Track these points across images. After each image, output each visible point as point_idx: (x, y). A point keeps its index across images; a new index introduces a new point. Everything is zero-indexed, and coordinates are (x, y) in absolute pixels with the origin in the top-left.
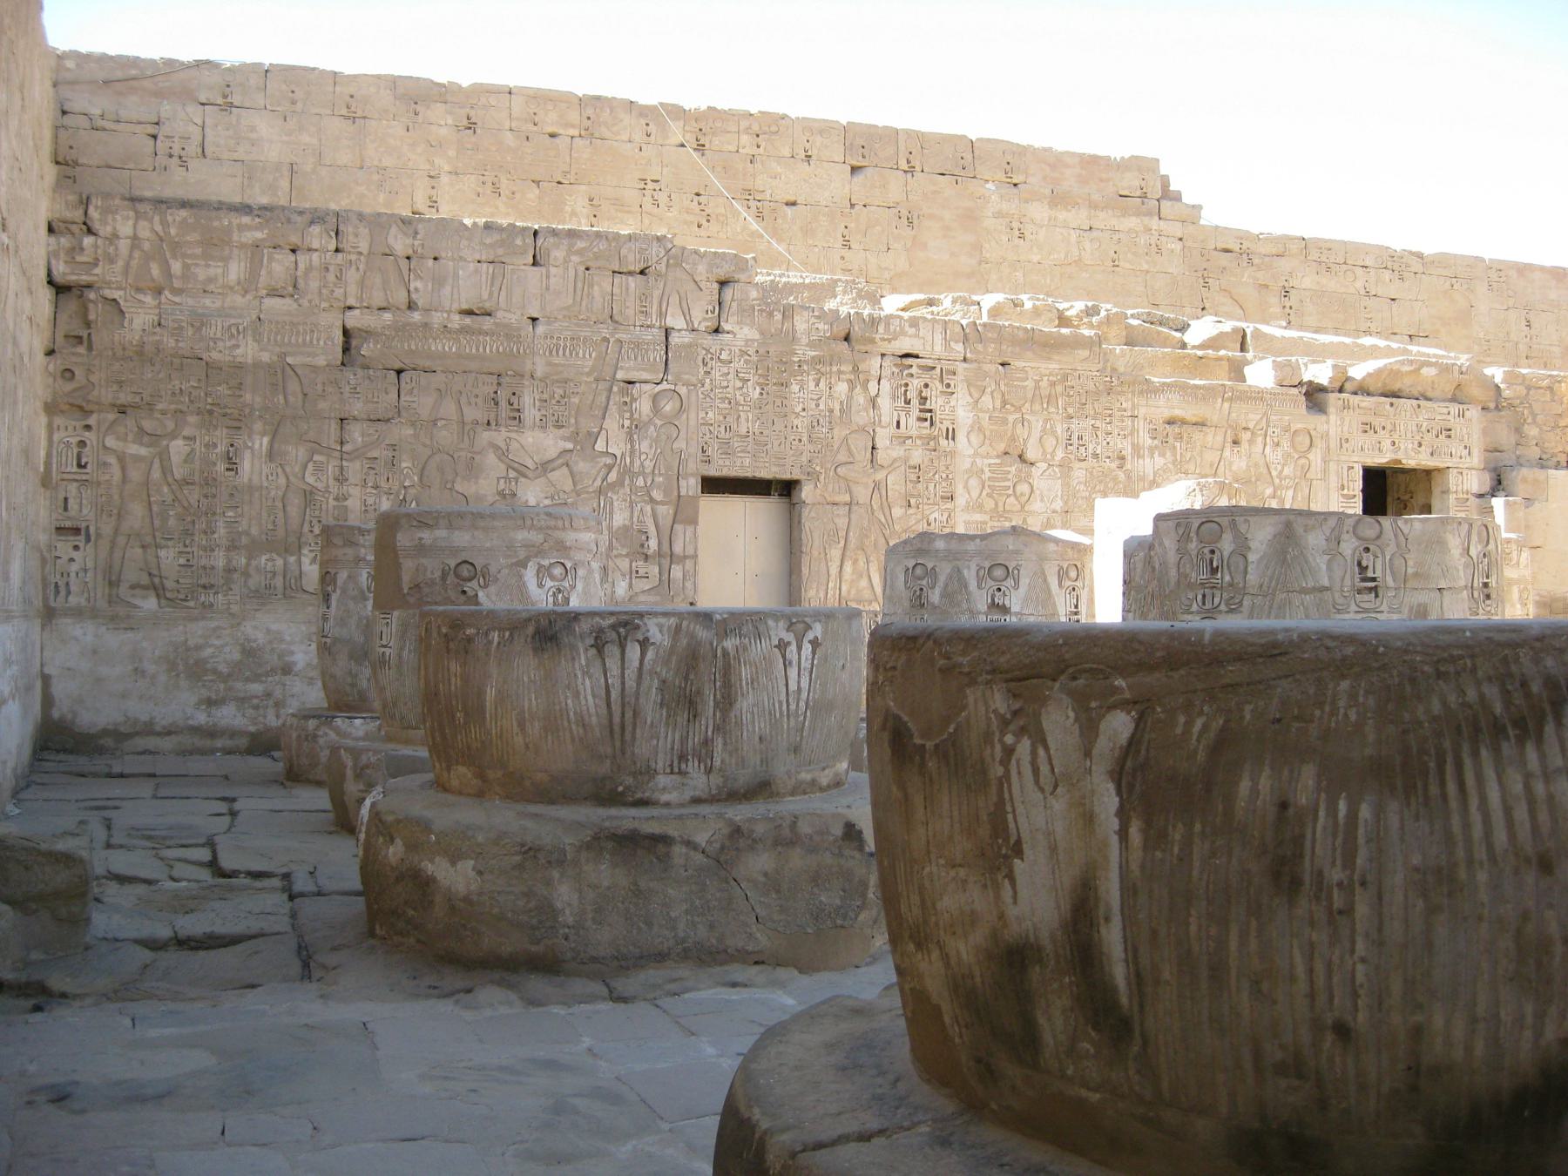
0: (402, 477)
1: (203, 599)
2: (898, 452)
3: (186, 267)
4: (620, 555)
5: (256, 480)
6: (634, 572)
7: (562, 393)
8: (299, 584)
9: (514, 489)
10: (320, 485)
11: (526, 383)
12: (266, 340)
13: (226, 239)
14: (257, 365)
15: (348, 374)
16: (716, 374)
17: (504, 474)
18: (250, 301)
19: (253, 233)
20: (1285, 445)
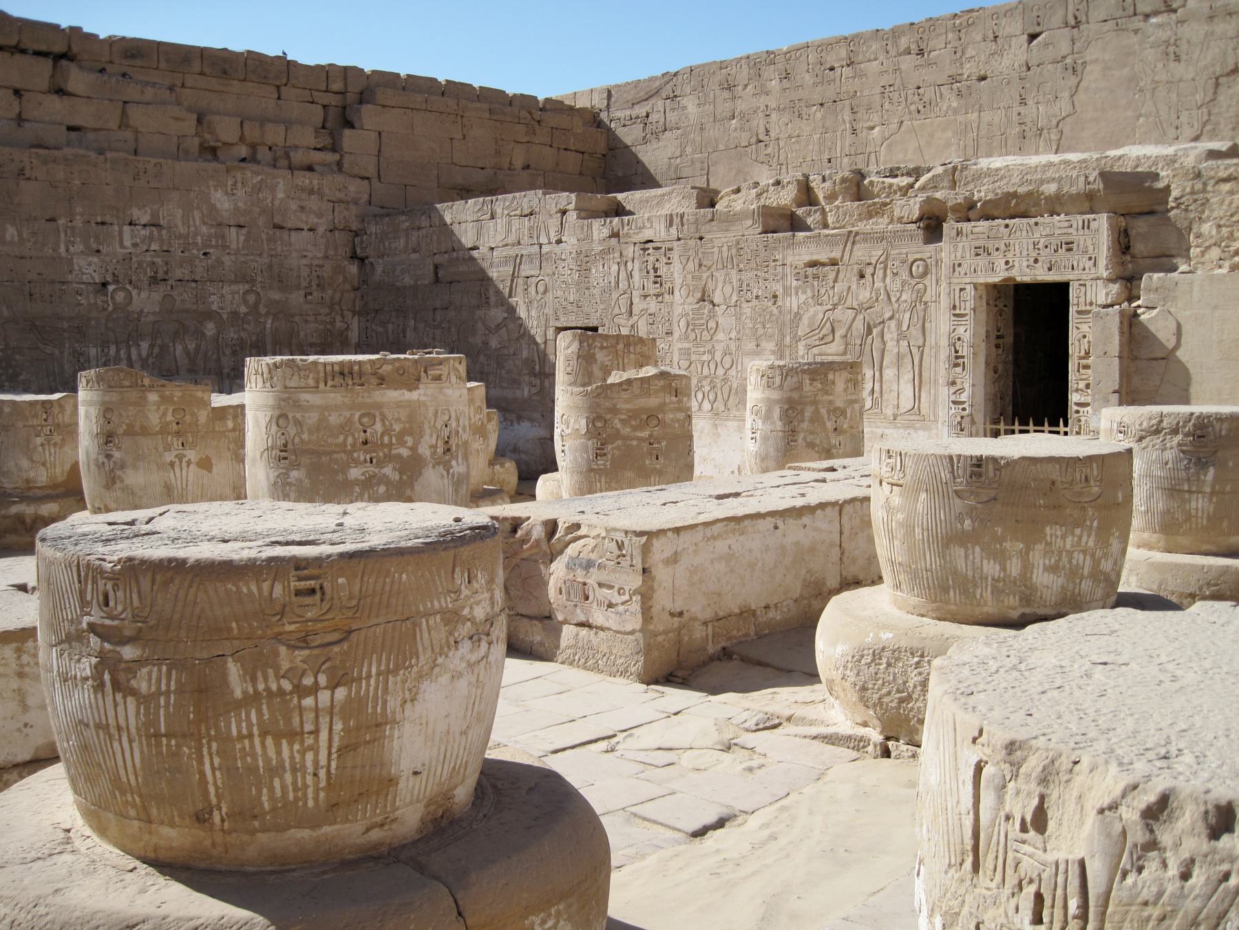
2: (643, 305)
16: (560, 268)
20: (904, 275)
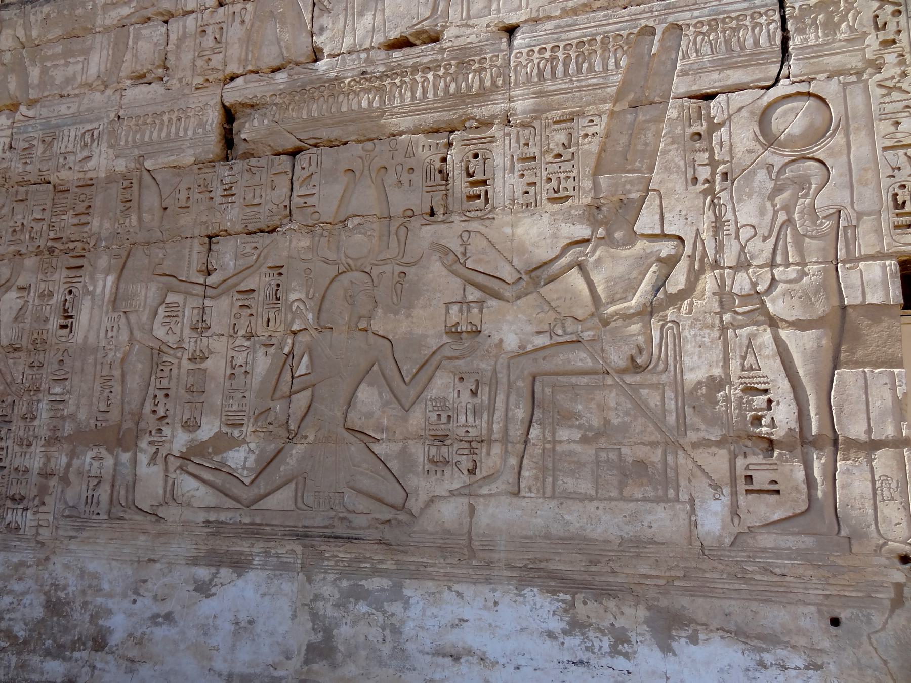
0: (290, 316)
1: (9, 518)
3: (44, 71)
4: (704, 443)
5: (92, 340)
6: (741, 482)
7: (561, 137)
8: (130, 498)
9: (476, 321)
10: (171, 340)
11: (498, 134)
12: (122, 143)
13: (89, 26)
14: (111, 178)
15: (223, 170)
17: (459, 299)
18: (109, 97)
19: (119, 10)
